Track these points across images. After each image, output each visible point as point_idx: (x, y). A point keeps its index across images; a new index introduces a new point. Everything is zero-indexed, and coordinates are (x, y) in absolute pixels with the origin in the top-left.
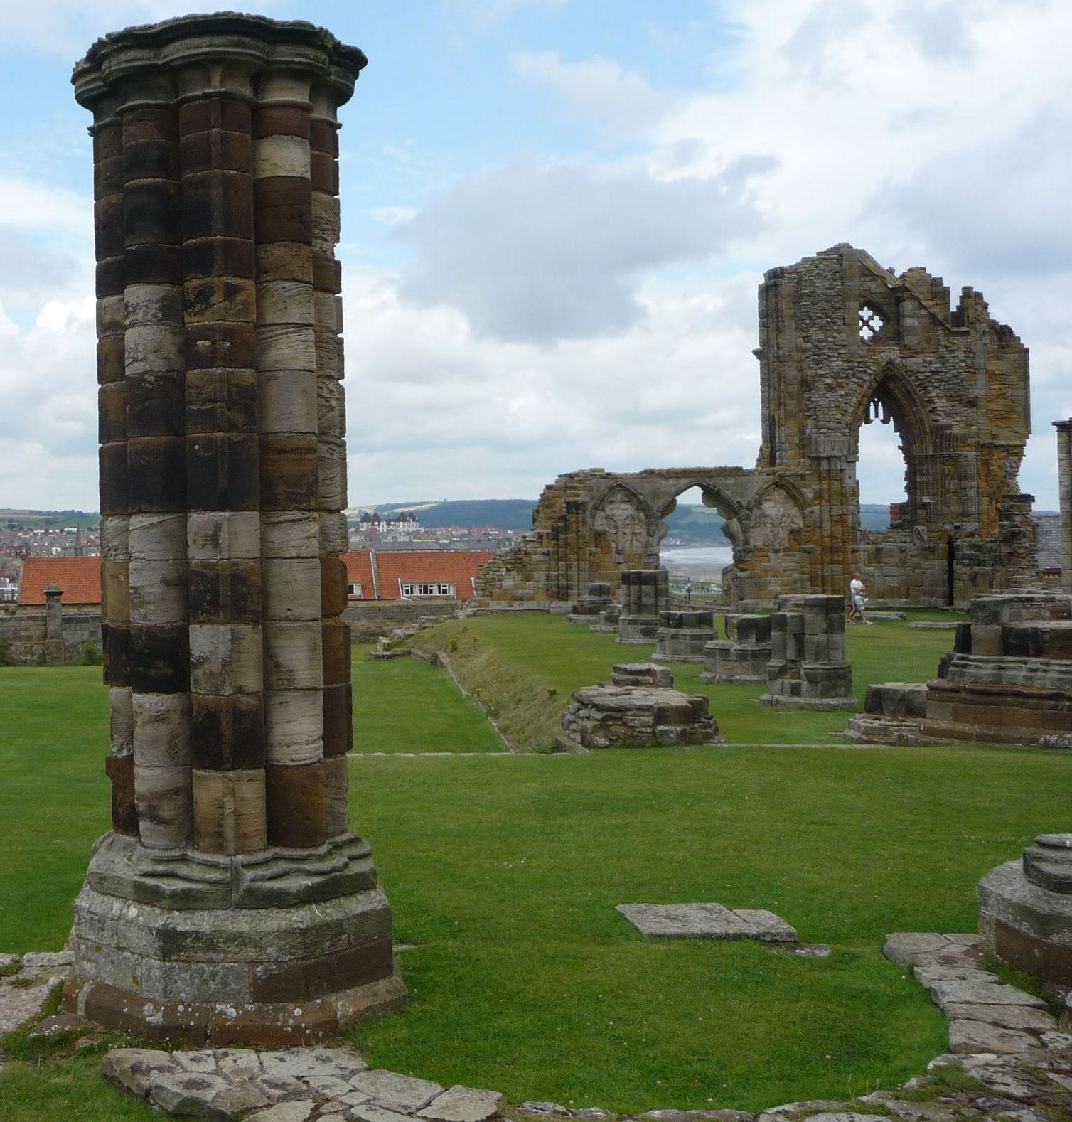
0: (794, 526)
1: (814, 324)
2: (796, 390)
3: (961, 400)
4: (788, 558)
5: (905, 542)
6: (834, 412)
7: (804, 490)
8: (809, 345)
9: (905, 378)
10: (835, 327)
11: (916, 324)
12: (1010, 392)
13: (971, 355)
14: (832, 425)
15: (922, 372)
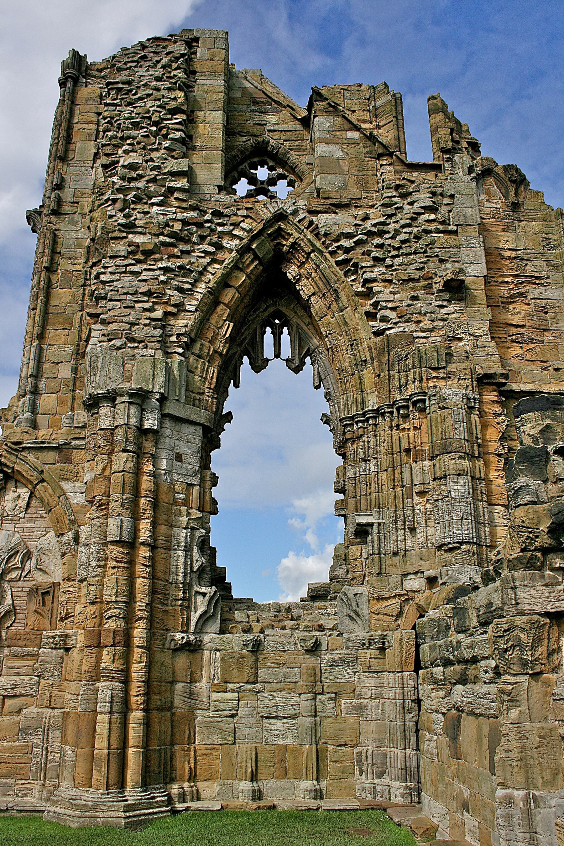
0: (40, 578)
1: (123, 139)
2: (79, 267)
3: (430, 286)
4: (18, 663)
5: (321, 628)
6: (147, 305)
7: (67, 486)
8: (115, 179)
9: (315, 249)
10: (166, 144)
11: (339, 154)
12: (534, 291)
13: (446, 201)
14: (139, 332)
15: (349, 236)
